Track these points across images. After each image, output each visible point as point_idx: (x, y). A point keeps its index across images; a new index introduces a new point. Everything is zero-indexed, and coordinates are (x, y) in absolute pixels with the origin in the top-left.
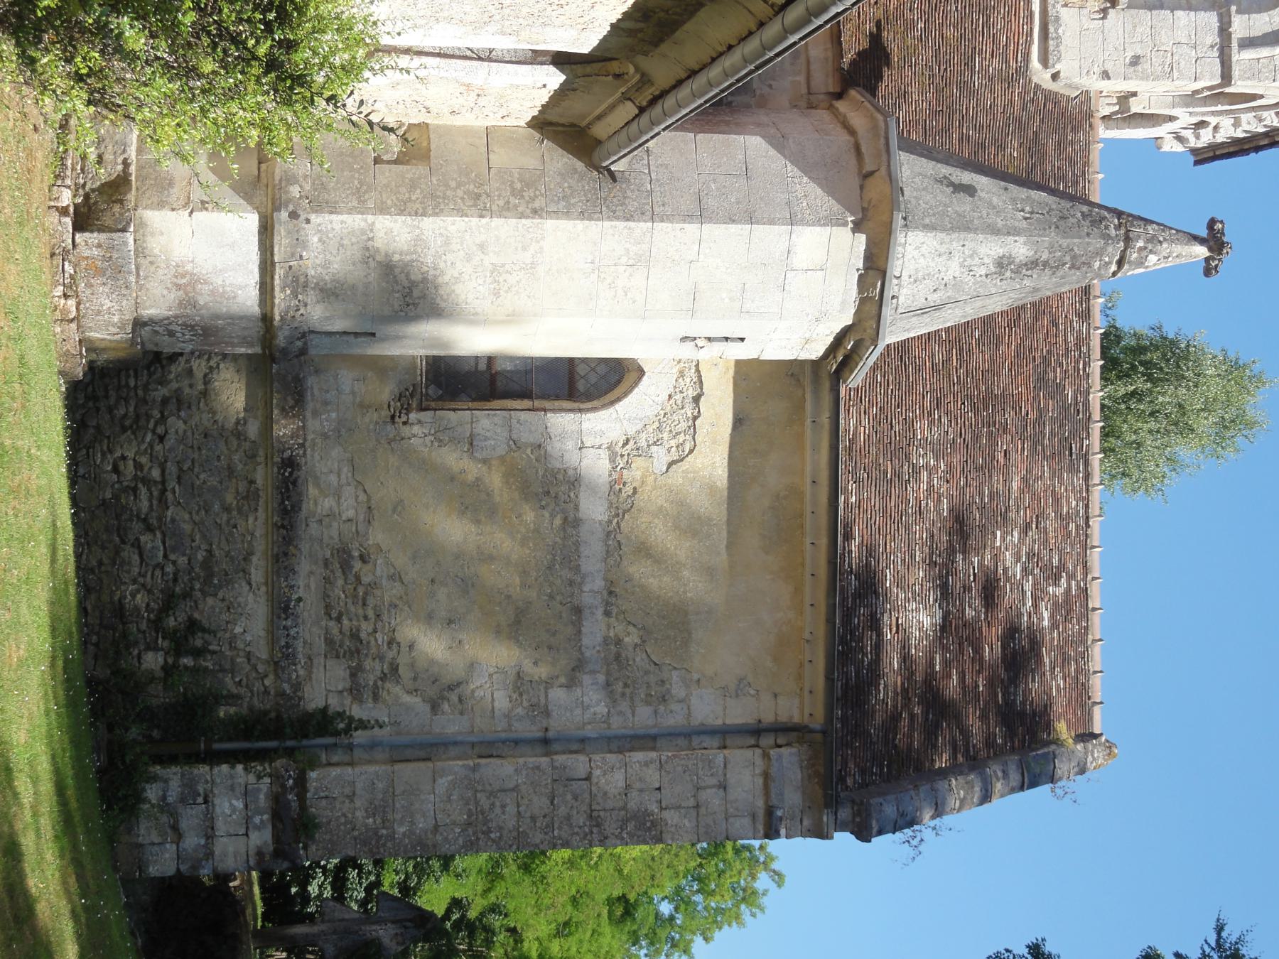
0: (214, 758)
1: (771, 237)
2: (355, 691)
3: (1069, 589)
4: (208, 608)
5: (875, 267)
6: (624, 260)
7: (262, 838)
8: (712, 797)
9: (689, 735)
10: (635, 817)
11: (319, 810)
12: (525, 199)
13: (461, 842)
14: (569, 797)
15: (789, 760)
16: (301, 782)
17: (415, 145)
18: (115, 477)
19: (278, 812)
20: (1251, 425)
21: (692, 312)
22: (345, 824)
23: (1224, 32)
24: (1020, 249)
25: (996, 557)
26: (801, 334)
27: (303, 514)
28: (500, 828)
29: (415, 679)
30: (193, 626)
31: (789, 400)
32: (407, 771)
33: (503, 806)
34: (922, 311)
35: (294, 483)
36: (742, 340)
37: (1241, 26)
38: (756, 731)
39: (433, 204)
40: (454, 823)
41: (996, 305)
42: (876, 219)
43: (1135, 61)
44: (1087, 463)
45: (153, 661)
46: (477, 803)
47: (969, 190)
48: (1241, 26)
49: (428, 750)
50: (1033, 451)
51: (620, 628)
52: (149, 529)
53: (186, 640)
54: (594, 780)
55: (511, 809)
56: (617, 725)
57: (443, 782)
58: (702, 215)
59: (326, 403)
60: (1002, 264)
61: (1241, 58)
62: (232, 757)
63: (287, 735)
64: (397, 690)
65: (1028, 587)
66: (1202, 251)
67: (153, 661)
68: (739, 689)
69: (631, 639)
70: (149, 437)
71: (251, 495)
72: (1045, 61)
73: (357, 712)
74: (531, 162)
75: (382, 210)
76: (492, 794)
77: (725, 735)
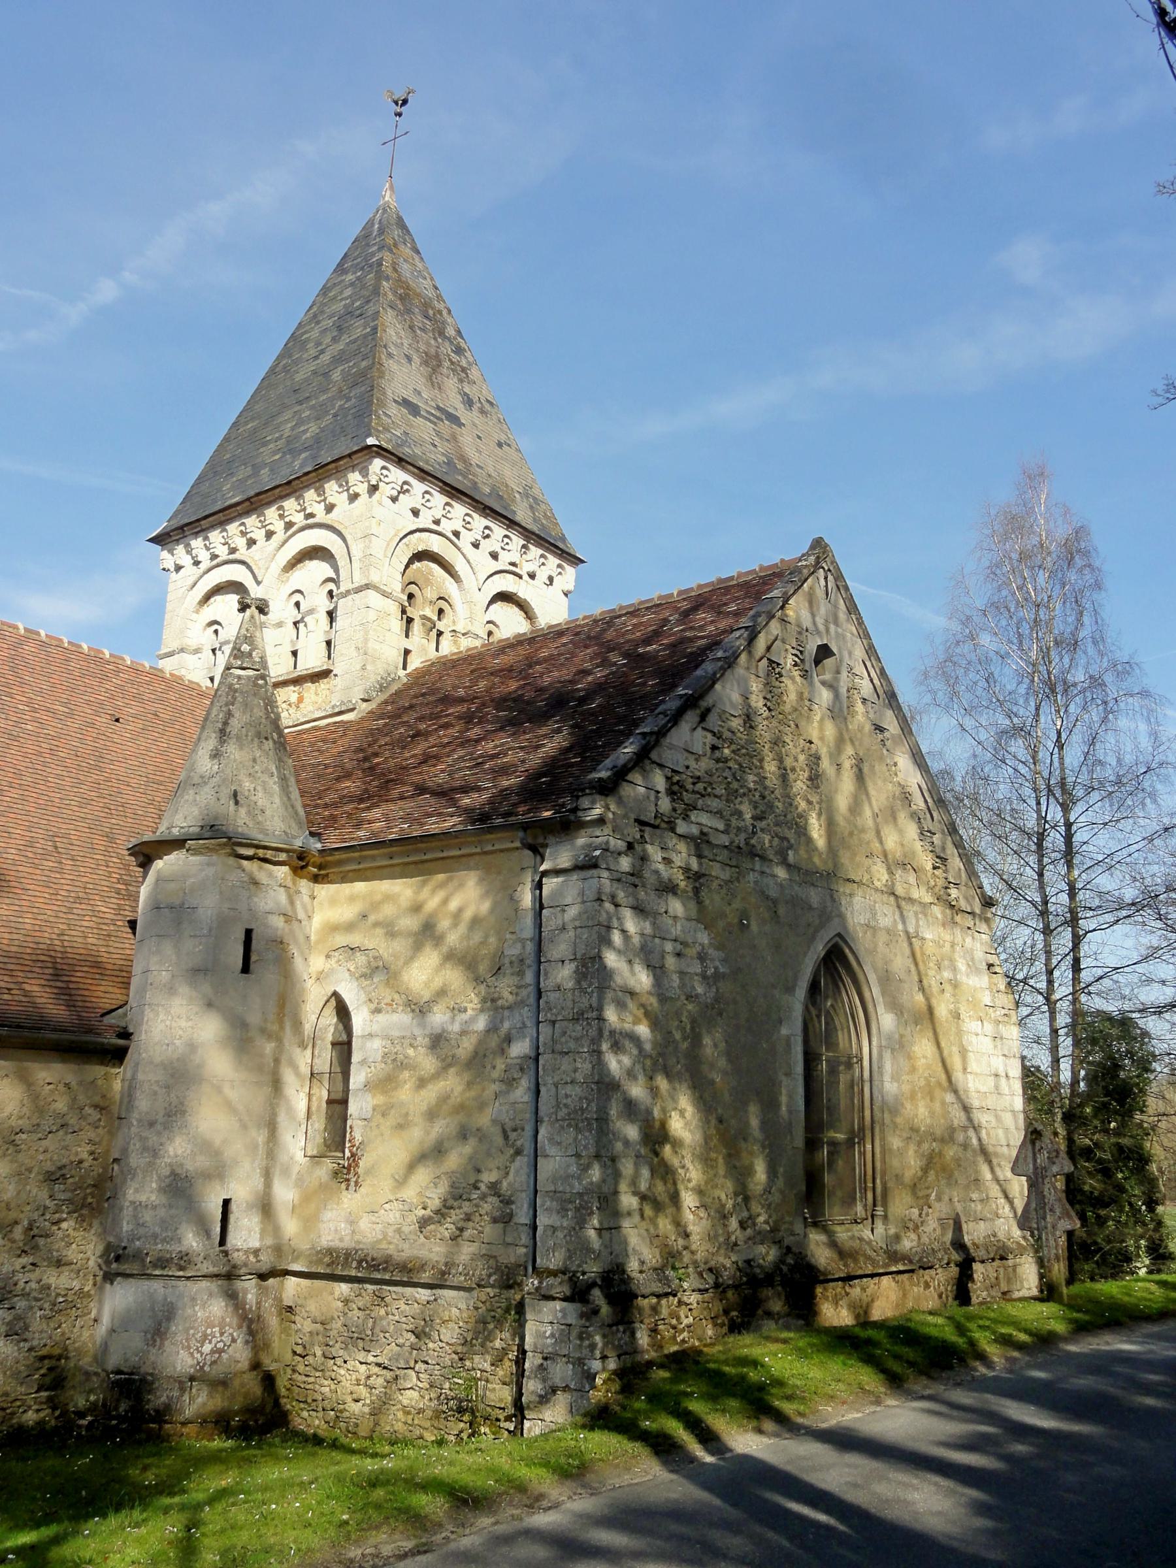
6: (168, 1023)
10: (578, 982)
13: (587, 1134)
14: (563, 1039)
18: (360, 1404)
22: (571, 1236)
27: (395, 1255)
28: (580, 1098)
29: (498, 1168)
33: (567, 1096)
35: (373, 1259)
36: (249, 933)
40: (575, 1139)
46: (563, 1120)
54: (553, 1018)
55: (569, 1089)
59: (336, 1230)
61: (359, 580)
64: (505, 1184)
70: (342, 1372)
76: (558, 1106)
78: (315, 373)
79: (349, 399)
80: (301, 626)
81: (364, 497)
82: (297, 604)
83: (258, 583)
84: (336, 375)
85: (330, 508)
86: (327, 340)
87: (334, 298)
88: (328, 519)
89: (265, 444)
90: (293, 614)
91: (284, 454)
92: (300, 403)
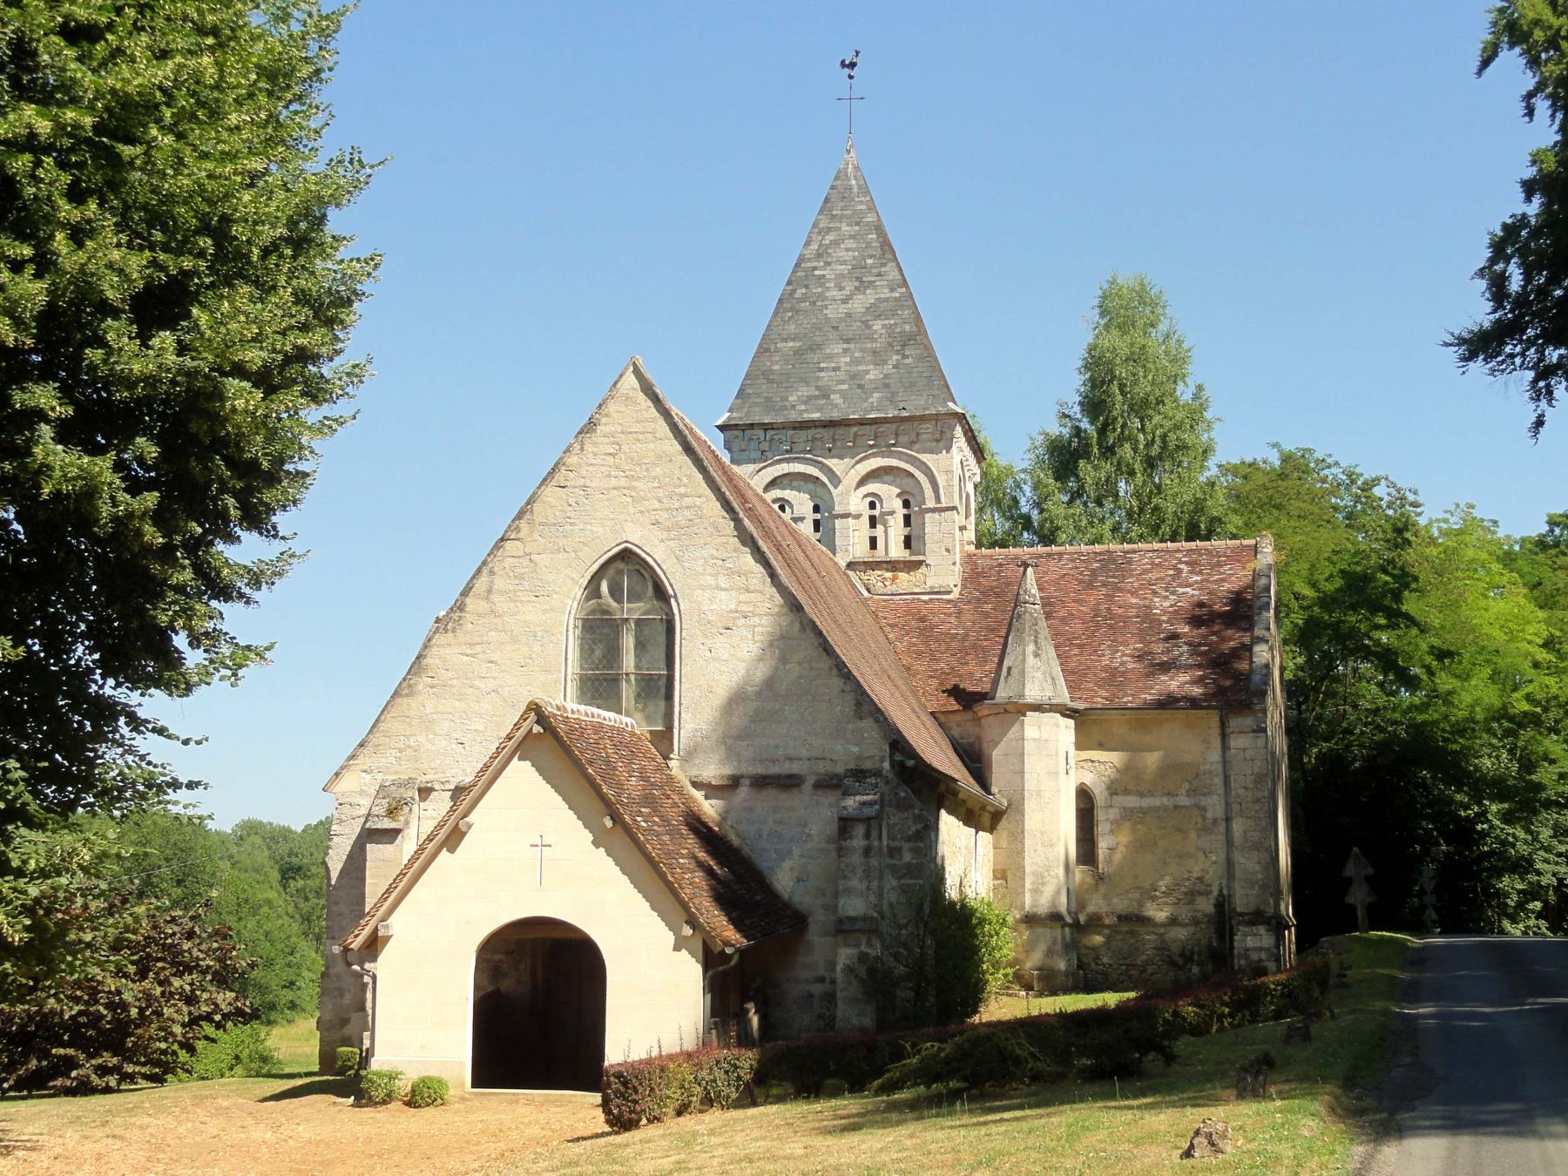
0: (1232, 948)
1: (1029, 747)
2: (1207, 893)
3: (1186, 563)
4: (1175, 949)
5: (1038, 708)
7: (1262, 930)
8: (1249, 754)
9: (1225, 763)
11: (1252, 909)
12: (1018, 836)
15: (1234, 723)
16: (1241, 914)
17: (1001, 874)
19: (1252, 923)
20: (1142, 284)
21: (1057, 773)
23: (933, 510)
24: (1031, 648)
25: (1165, 612)
26: (1065, 730)
30: (1182, 955)
31: (1090, 726)
32: (1238, 874)
34: (1054, 684)
37: (930, 504)
38: (1224, 735)
39: (1021, 868)
41: (1052, 653)
42: (1019, 710)
43: (948, 550)
44: (1128, 552)
45: (1195, 970)
47: (1009, 669)
48: (930, 504)
49: (1230, 864)
50: (1120, 590)
51: (1183, 791)
52: (1144, 971)
53: (1187, 956)
56: (1221, 791)
57: (1242, 860)
58: (1022, 772)
60: (1036, 655)
62: (1232, 941)
63: (1224, 919)
65: (1181, 590)
66: (1030, 570)
67: (1195, 970)
68: (1206, 742)
69: (1187, 785)
71: (1132, 933)
72: (949, 593)
73: (1216, 893)
74: (1005, 833)
75: (1023, 886)
77: (1225, 747)
78: (849, 315)
79: (904, 357)
82: (872, 506)
84: (877, 326)
86: (849, 287)
87: (836, 243)
89: (821, 370)
90: (867, 512)
92: (847, 341)
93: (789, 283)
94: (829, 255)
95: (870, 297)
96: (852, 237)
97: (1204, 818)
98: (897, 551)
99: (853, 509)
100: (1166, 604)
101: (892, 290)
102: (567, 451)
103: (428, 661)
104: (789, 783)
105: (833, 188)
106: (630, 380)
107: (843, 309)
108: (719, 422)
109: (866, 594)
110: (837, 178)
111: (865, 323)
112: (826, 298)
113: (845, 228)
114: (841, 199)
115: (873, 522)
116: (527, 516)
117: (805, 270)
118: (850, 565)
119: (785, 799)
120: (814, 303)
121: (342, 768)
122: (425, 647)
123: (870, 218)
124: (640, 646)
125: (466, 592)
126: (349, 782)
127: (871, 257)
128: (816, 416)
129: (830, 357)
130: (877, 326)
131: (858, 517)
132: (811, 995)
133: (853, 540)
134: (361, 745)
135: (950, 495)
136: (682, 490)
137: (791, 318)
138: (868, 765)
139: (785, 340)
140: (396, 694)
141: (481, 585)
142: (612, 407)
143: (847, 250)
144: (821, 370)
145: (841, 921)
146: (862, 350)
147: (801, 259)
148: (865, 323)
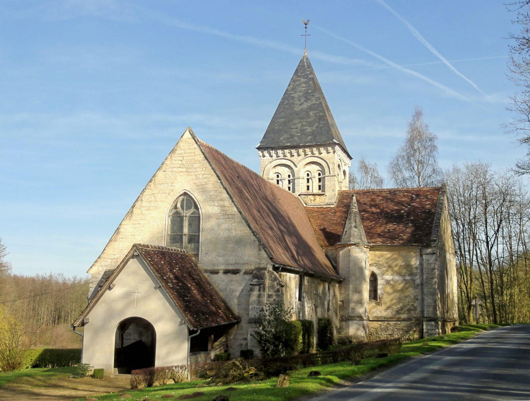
23: (328, 176)
38: (421, 255)
47: (346, 232)
48: (327, 174)
57: (427, 299)
77: (422, 260)
78: (302, 110)
79: (320, 124)
80: (310, 180)
81: (332, 153)
82: (308, 175)
83: (296, 166)
84: (311, 113)
85: (320, 154)
86: (303, 100)
87: (299, 85)
88: (320, 156)
89: (292, 128)
90: (306, 177)
91: (301, 135)
92: (301, 119)
93: (282, 99)
94: (296, 89)
95: (309, 104)
96: (304, 83)
97: (414, 284)
98: (316, 191)
99: (301, 176)
100: (406, 209)
101: (317, 101)
102: (166, 159)
103: (121, 230)
104: (235, 272)
105: (298, 66)
106: (187, 135)
107: (300, 107)
108: (257, 147)
109: (305, 205)
110: (300, 62)
111: (307, 112)
112: (295, 104)
113: (302, 80)
114: (304, 70)
115: (308, 182)
116: (153, 181)
117: (288, 94)
118: (299, 195)
119: (233, 277)
120: (290, 106)
121: (93, 265)
122: (120, 225)
123: (311, 76)
124: (190, 225)
125: (133, 207)
126: (94, 270)
127: (310, 89)
128: (289, 144)
129: (295, 124)
130: (311, 113)
131: (303, 178)
132: (242, 344)
133: (301, 187)
134: (99, 258)
135: (334, 171)
136: (203, 172)
137: (282, 111)
138: (262, 266)
139: (280, 119)
140: (110, 240)
141: (138, 204)
142: (181, 144)
143: (303, 87)
144: (292, 128)
145: (250, 319)
146: (306, 122)
147: (287, 90)
148: (307, 112)
